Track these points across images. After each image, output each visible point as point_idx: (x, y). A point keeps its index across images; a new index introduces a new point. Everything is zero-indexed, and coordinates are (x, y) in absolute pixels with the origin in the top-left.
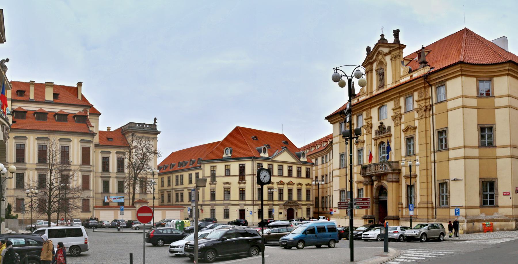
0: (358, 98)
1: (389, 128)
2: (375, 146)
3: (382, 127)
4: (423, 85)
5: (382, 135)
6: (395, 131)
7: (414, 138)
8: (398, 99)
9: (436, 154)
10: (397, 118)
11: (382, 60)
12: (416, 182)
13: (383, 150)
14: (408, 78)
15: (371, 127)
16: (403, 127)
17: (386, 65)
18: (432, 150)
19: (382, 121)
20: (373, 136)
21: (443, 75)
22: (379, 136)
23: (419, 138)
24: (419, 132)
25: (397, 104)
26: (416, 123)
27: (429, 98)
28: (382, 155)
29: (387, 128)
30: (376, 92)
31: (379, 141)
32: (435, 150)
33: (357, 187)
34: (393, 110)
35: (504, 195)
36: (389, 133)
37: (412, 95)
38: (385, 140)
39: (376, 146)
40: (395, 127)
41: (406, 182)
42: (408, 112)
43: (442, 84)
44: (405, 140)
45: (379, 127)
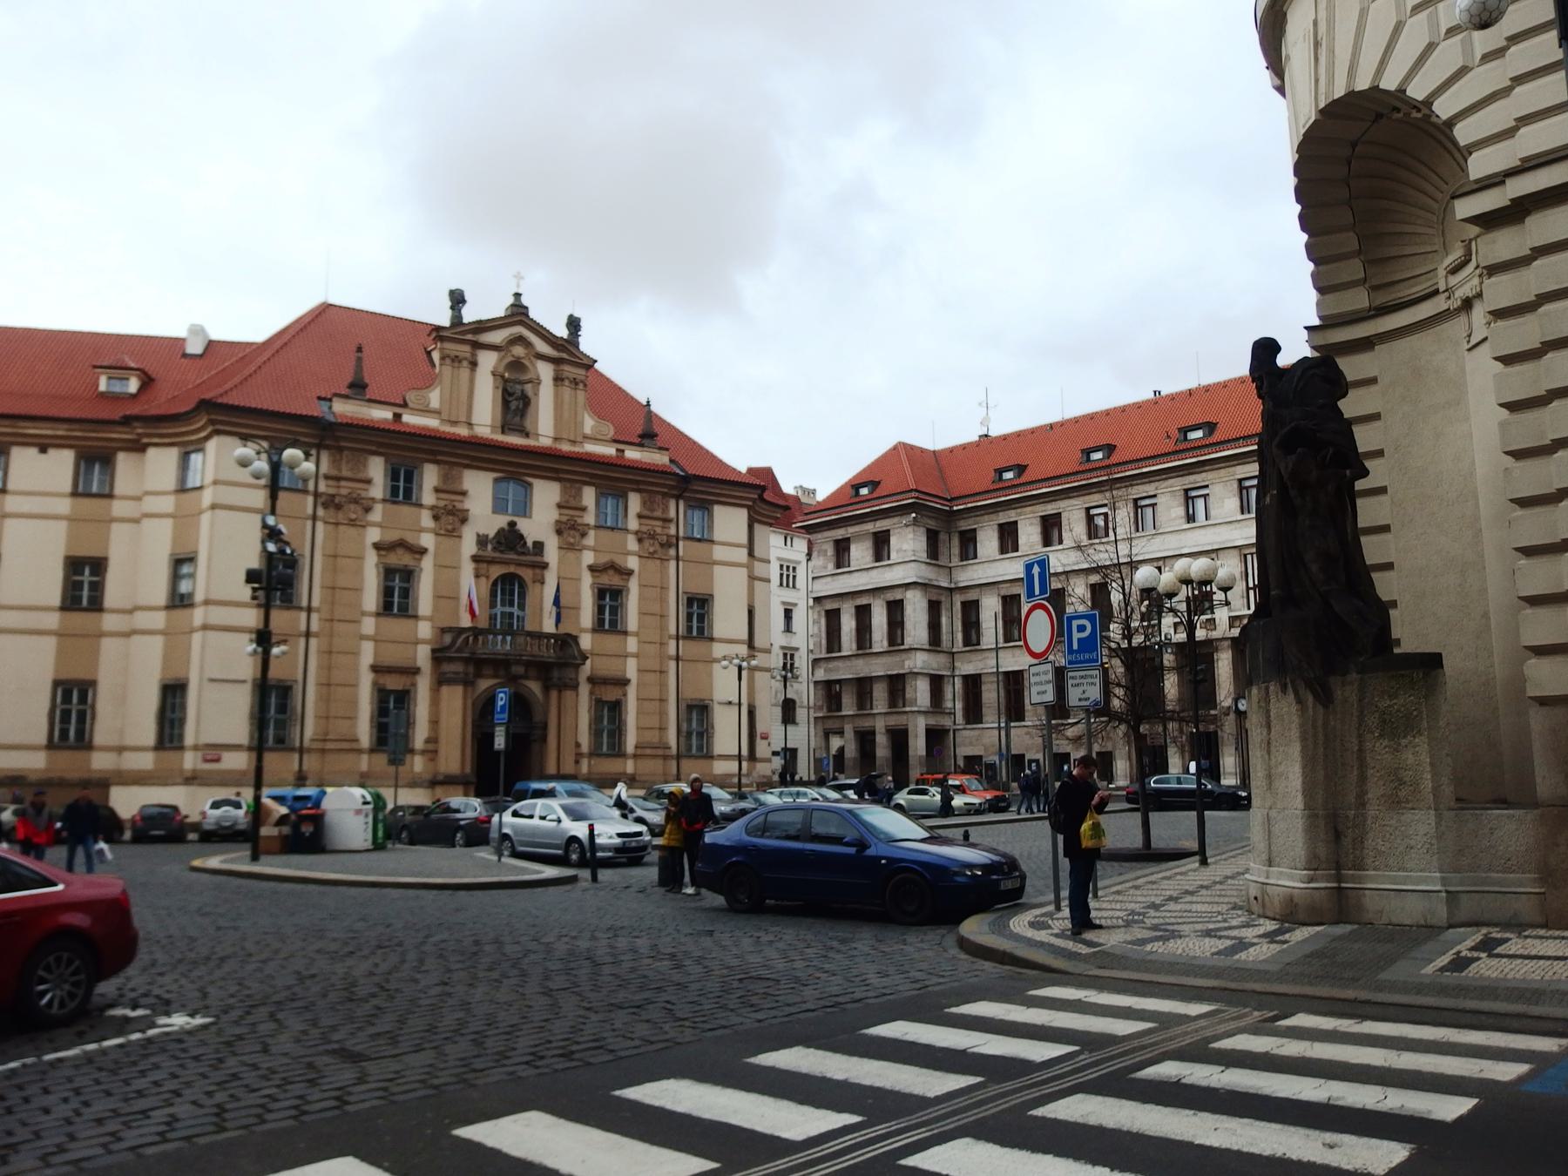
0: (398, 410)
1: (539, 546)
2: (477, 576)
3: (510, 539)
4: (666, 490)
5: (513, 556)
6: (560, 561)
7: (624, 593)
8: (577, 485)
9: (681, 642)
10: (569, 530)
11: (526, 362)
12: (625, 695)
13: (502, 594)
14: (610, 451)
15: (464, 520)
16: (588, 558)
17: (539, 384)
18: (673, 631)
19: (515, 519)
20: (469, 546)
21: (718, 491)
22: (497, 555)
23: (642, 598)
24: (641, 586)
25: (575, 498)
26: (633, 563)
27: (670, 521)
28: (499, 609)
29: (530, 544)
30: (492, 432)
31: (496, 571)
32: (680, 633)
33: (375, 684)
34: (559, 506)
35: (762, 738)
36: (538, 559)
37: (622, 496)
38: (527, 574)
39: (483, 580)
40: (563, 552)
41: (591, 693)
42: (608, 528)
43: (705, 506)
44: (593, 591)
45: (500, 532)
